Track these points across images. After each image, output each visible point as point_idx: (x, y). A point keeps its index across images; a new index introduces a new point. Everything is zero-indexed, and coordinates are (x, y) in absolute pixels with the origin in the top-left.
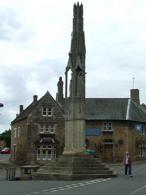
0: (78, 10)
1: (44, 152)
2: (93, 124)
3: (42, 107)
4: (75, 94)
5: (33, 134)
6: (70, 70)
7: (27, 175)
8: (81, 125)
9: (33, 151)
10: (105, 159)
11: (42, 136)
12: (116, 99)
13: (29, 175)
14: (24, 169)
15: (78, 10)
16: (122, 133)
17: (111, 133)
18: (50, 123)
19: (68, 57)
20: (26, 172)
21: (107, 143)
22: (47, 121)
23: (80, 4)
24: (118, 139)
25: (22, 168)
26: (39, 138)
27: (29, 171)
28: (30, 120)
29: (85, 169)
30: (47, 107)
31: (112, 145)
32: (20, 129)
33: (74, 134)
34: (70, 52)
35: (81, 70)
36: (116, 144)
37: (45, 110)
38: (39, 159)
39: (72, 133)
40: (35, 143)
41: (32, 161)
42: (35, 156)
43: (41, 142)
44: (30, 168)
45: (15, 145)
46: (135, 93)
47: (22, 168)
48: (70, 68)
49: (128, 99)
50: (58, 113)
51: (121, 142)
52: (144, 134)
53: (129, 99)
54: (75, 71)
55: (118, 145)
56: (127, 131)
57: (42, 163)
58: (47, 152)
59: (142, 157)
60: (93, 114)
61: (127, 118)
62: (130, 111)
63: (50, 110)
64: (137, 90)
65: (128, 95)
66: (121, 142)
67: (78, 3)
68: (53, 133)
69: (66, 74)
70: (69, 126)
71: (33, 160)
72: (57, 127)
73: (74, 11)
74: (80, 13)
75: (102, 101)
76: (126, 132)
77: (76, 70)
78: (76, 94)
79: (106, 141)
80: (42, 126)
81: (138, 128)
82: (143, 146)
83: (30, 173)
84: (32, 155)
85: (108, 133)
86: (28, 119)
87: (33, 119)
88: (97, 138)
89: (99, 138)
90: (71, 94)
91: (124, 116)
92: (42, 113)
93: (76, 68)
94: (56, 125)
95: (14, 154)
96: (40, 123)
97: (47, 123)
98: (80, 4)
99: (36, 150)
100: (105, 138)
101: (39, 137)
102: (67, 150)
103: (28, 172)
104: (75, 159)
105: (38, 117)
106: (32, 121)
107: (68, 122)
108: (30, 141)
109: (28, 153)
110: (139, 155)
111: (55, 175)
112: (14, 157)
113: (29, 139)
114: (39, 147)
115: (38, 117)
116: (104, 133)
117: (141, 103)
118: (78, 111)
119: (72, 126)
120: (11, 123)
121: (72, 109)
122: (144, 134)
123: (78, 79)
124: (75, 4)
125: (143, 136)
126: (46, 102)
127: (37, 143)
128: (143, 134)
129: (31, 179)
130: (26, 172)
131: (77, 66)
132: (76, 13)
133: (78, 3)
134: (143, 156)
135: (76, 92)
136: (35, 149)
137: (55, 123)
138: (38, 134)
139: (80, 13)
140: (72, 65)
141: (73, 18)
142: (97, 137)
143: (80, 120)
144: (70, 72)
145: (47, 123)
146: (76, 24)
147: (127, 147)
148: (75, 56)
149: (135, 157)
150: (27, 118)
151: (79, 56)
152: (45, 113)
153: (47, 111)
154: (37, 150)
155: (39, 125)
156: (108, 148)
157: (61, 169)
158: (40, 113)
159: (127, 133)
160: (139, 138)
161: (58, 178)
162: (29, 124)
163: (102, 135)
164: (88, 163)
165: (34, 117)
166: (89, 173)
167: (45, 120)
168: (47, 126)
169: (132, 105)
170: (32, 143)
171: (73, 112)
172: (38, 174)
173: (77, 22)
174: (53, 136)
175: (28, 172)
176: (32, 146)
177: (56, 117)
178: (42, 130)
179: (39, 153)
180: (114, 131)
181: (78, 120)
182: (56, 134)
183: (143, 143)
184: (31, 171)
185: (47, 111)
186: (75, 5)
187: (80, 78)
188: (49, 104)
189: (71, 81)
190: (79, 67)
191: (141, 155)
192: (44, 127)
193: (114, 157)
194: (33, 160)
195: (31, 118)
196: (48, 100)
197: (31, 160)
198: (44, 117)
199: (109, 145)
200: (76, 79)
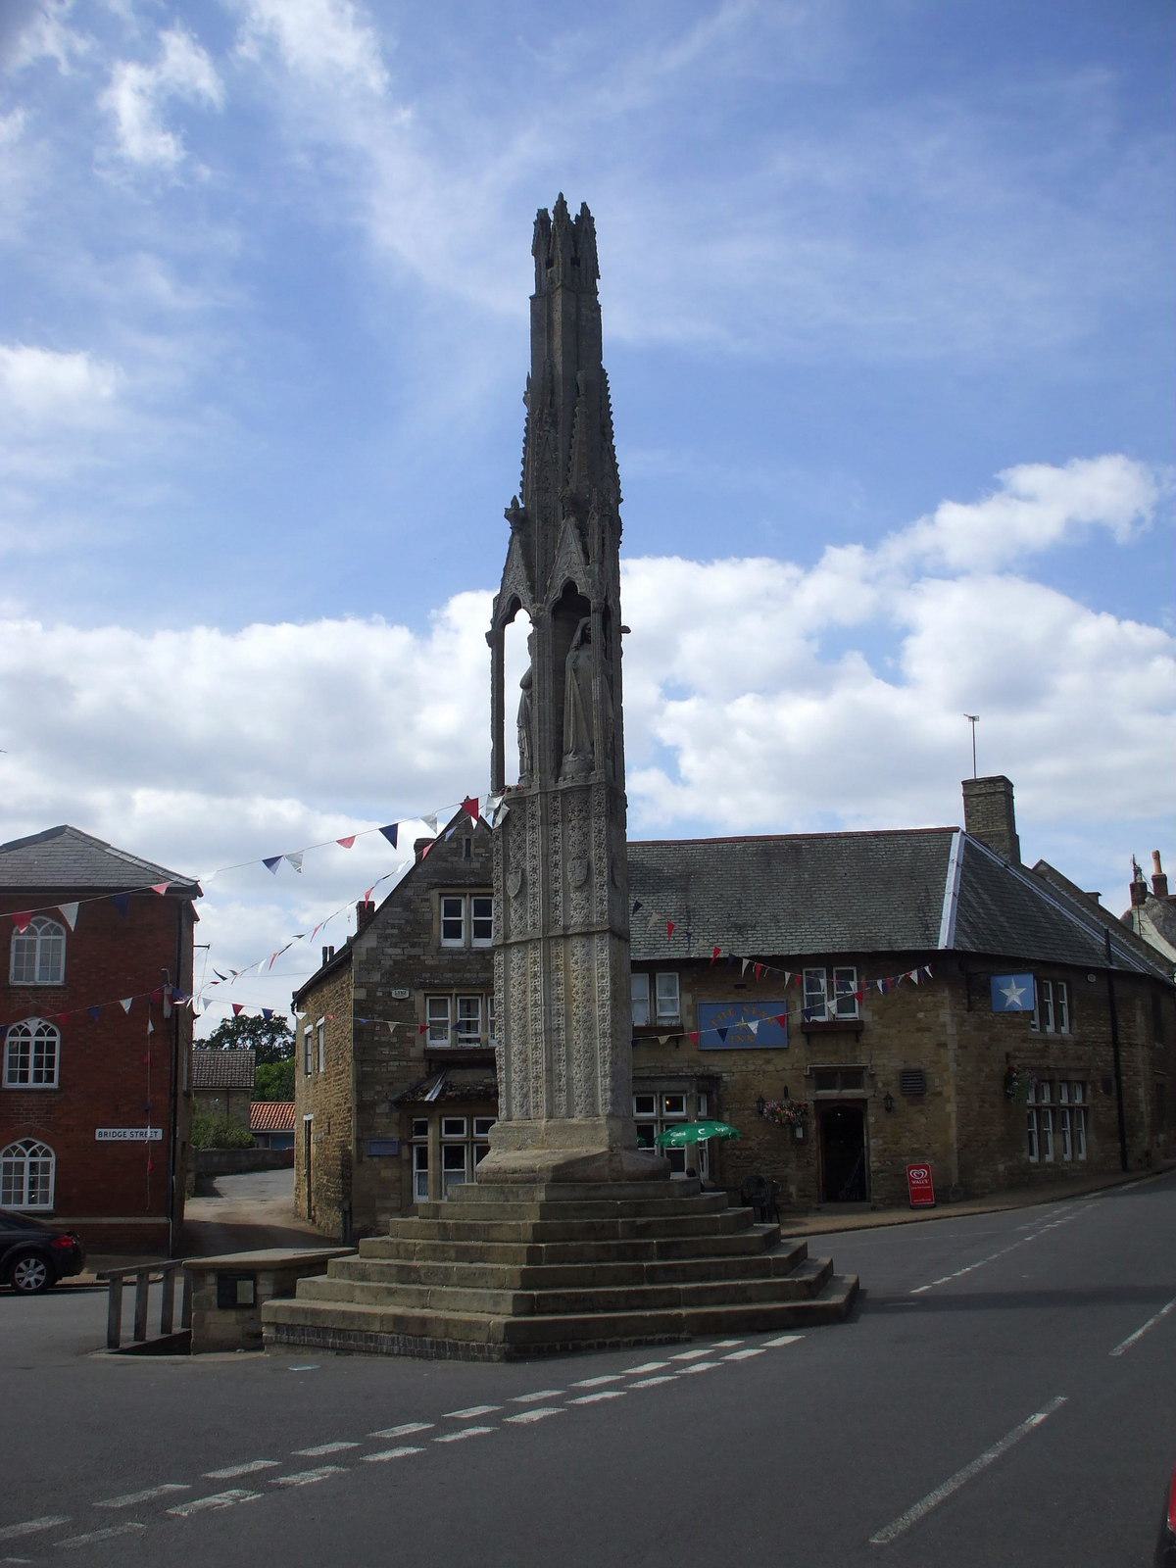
0: (566, 250)
2: (743, 986)
3: (435, 893)
4: (549, 764)
6: (522, 616)
7: (232, 1316)
8: (589, 969)
9: (391, 1152)
12: (877, 834)
13: (248, 1314)
14: (211, 1279)
15: (566, 250)
16: (919, 1030)
17: (855, 1030)
19: (505, 529)
20: (228, 1300)
22: (468, 975)
23: (574, 210)
24: (897, 1064)
25: (197, 1274)
26: (422, 1075)
29: (615, 1266)
30: (465, 895)
33: (548, 1031)
34: (514, 502)
35: (581, 606)
36: (888, 1098)
37: (453, 909)
39: (540, 1026)
40: (398, 1104)
42: (399, 1180)
43: (431, 1096)
44: (251, 1272)
45: (310, 1121)
46: (991, 799)
47: (197, 1274)
48: (516, 605)
49: (946, 833)
51: (914, 1084)
52: (1050, 1029)
53: (956, 830)
54: (547, 614)
56: (945, 1016)
59: (1049, 1165)
60: (740, 929)
61: (943, 941)
62: (961, 899)
64: (1003, 779)
65: (947, 811)
66: (914, 1084)
67: (561, 204)
69: (496, 640)
70: (518, 982)
71: (390, 1204)
73: (535, 252)
74: (575, 261)
76: (944, 1025)
77: (558, 608)
78: (559, 764)
79: (823, 1078)
80: (439, 1007)
81: (1016, 993)
82: (1046, 1101)
84: (387, 1173)
85: (834, 1029)
87: (387, 963)
88: (770, 1068)
89: (780, 1062)
90: (526, 770)
91: (930, 929)
92: (439, 929)
93: (555, 594)
95: (309, 1173)
96: (423, 986)
97: (469, 986)
98: (574, 210)
99: (405, 1150)
100: (823, 1062)
101: (420, 1070)
102: (504, 1144)
103: (240, 1300)
104: (546, 1210)
106: (376, 977)
107: (515, 956)
108: (368, 1096)
109: (360, 1162)
110: (1026, 1155)
111: (398, 1320)
112: (309, 1186)
113: (362, 1082)
114: (422, 1129)
116: (812, 1032)
117: (1028, 860)
118: (574, 876)
119: (539, 982)
120: (294, 994)
121: (534, 870)
122: (1050, 1029)
123: (569, 664)
124: (542, 215)
125: (1047, 1042)
126: (461, 863)
127: (408, 1106)
128: (1043, 1030)
129: (253, 1341)
131: (559, 583)
132: (549, 264)
133: (561, 204)
134: (1049, 1158)
135: (559, 752)
136: (402, 1142)
139: (575, 261)
140: (530, 578)
141: (533, 292)
142: (768, 1062)
143: (587, 935)
144: (521, 627)
145: (469, 986)
146: (550, 323)
147: (951, 1108)
148: (545, 520)
149: (1001, 1167)
151: (573, 519)
152: (453, 931)
153: (466, 915)
154: (411, 1145)
155: (418, 997)
157: (445, 1278)
158: (427, 926)
159: (951, 1030)
160: (1022, 1055)
161: (419, 1340)
162: (362, 994)
163: (798, 1048)
164: (642, 1231)
165: (390, 951)
166: (643, 1300)
169: (972, 860)
170: (383, 1108)
171: (538, 889)
172: (305, 1312)
173: (557, 316)
175: (240, 1300)
176: (386, 1123)
178: (438, 1030)
179: (423, 1164)
180: (868, 1017)
181: (576, 942)
183: (1051, 1082)
184: (261, 1290)
185: (466, 915)
186: (542, 218)
187: (585, 659)
188: (473, 873)
189: (526, 684)
190: (570, 587)
191: (1041, 1157)
192: (452, 1013)
194: (390, 1204)
198: (452, 951)
200: (559, 672)
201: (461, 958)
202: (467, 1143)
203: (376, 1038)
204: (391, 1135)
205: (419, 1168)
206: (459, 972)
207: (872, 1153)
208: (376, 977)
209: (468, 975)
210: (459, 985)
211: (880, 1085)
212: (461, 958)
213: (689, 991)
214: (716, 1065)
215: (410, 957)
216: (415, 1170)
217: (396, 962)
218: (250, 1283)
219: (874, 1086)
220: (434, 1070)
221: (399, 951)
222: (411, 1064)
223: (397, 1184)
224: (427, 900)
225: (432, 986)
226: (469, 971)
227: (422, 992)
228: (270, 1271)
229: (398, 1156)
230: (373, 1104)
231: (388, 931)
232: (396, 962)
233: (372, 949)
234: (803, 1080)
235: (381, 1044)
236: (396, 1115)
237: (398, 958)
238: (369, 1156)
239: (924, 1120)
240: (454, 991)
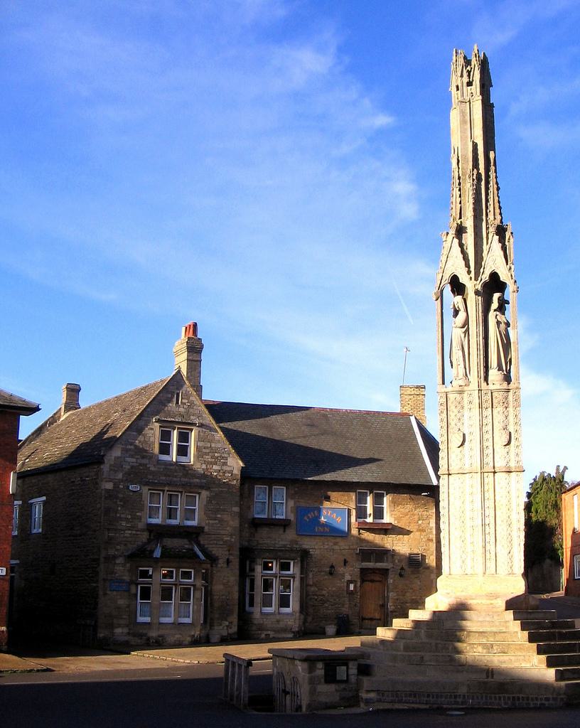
1: (166, 594)
5: (124, 524)
10: (363, 619)
11: (158, 533)
13: (343, 686)
14: (320, 665)
18: (183, 485)
20: (330, 677)
21: (371, 565)
22: (175, 479)
27: (341, 672)
28: (116, 471)
31: (385, 572)
32: (45, 503)
36: (402, 569)
38: (148, 619)
41: (119, 626)
42: (128, 606)
50: (214, 451)
55: (408, 570)
57: (161, 632)
58: (175, 594)
63: (184, 437)
68: (194, 523)
71: (122, 622)
72: (210, 500)
75: (325, 416)
83: (347, 681)
84: (121, 602)
86: (105, 468)
88: (336, 547)
93: (485, 277)
94: (205, 494)
96: (147, 484)
101: (144, 537)
105: (145, 461)
106: (120, 476)
108: (111, 552)
109: (105, 594)
115: (145, 461)
130: (330, 677)
137: (202, 487)
138: (141, 525)
142: (336, 544)
150: (100, 461)
154: (137, 585)
156: (372, 581)
162: (109, 486)
165: (129, 459)
167: (165, 475)
168: (171, 499)
174: (193, 534)
176: (122, 569)
177: (204, 466)
179: (146, 594)
182: (206, 529)
190: (494, 276)
193: (391, 612)
194: (122, 622)
195: (117, 466)
196: (177, 403)
197: (115, 621)
199: (374, 571)
201: (171, 467)
202: (176, 585)
203: (118, 515)
204: (125, 578)
205: (141, 599)
206: (169, 476)
207: (390, 601)
208: (120, 476)
209: (175, 479)
210: (169, 484)
211: (396, 561)
212: (171, 467)
213: (292, 499)
214: (307, 543)
215: (141, 464)
216: (139, 601)
217: (132, 467)
218: (344, 668)
219: (393, 562)
220: (152, 538)
221: (134, 460)
222: (139, 533)
223: (127, 609)
224: (152, 429)
225: (154, 484)
226: (176, 477)
227: (147, 488)
228: (321, 660)
229: (129, 591)
230: (115, 557)
231: (129, 447)
232: (132, 467)
233: (118, 458)
234: (355, 556)
235: (121, 519)
236: (128, 565)
237: (135, 464)
238: (111, 590)
239: (419, 583)
240: (166, 489)
